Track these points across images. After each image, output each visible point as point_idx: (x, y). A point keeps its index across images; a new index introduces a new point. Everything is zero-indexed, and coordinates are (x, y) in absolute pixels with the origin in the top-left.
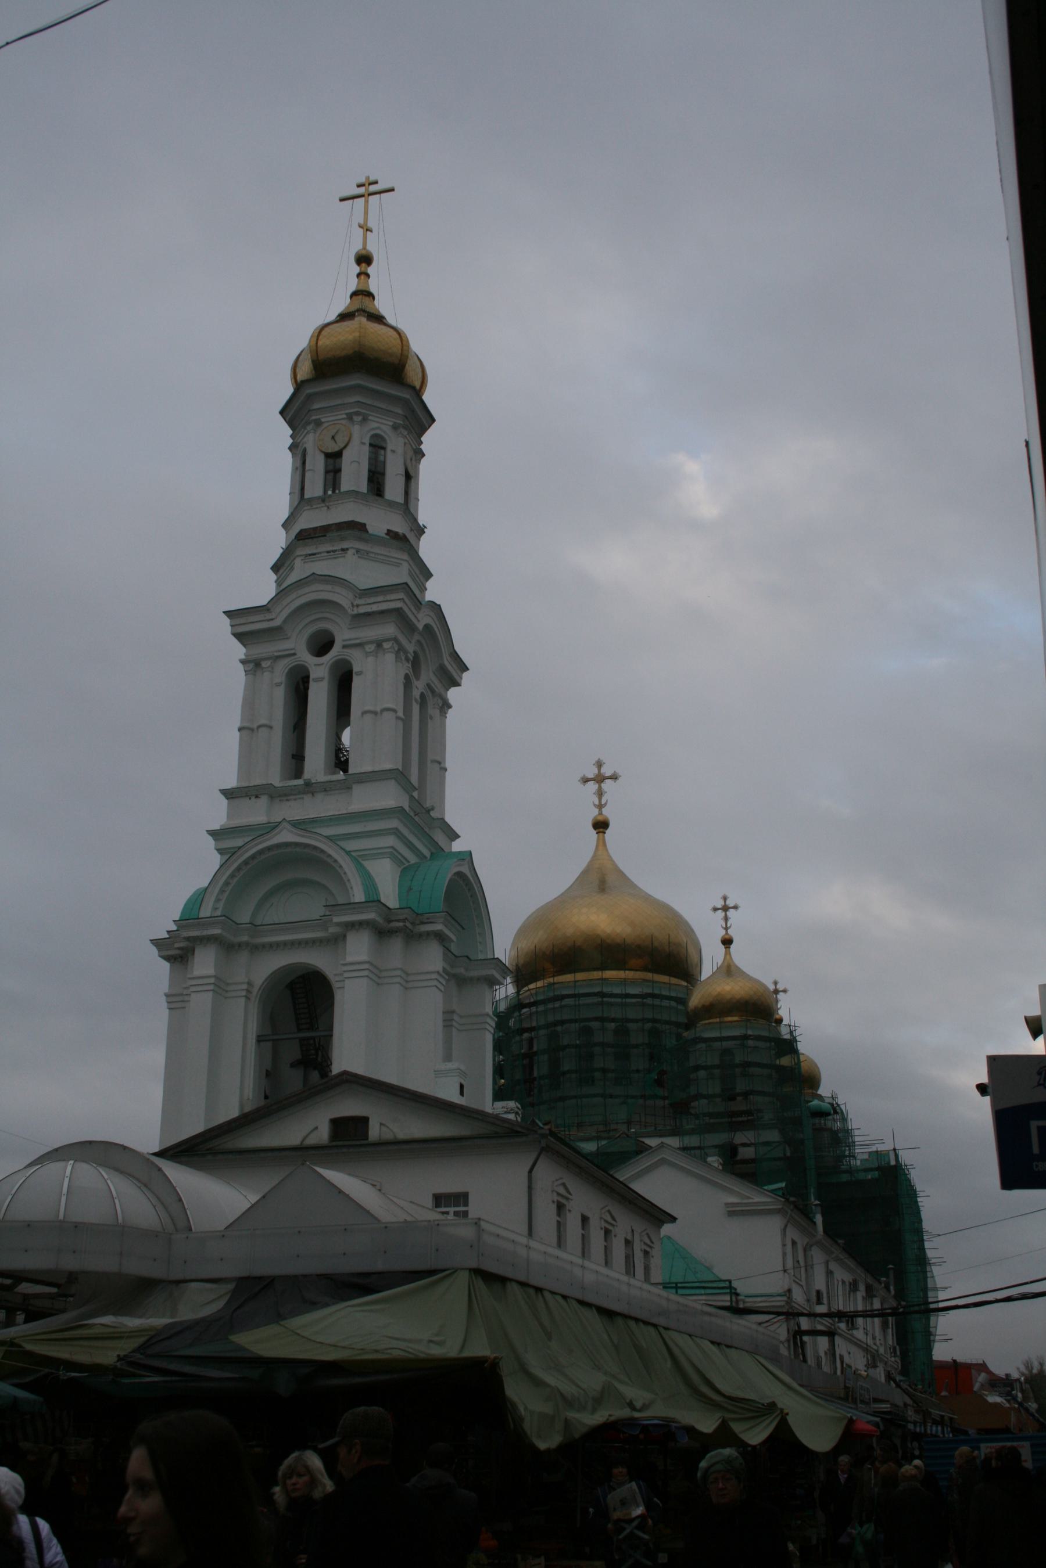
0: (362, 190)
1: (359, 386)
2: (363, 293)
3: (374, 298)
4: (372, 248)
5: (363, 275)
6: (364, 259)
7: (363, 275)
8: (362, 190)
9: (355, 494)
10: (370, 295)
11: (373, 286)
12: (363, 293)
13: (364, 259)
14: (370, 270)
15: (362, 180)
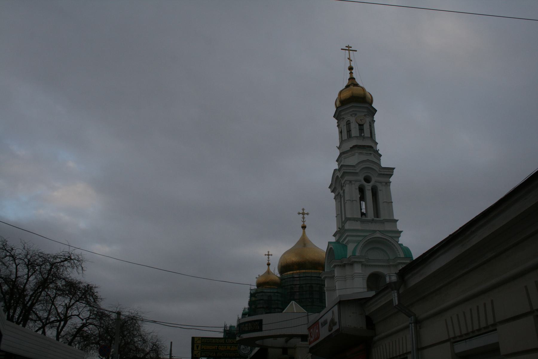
0: (347, 48)
1: (353, 106)
2: (352, 79)
3: (355, 79)
4: (353, 65)
5: (351, 73)
6: (351, 68)
7: (351, 73)
8: (347, 48)
9: (357, 137)
10: (354, 79)
11: (354, 76)
12: (352, 79)
13: (351, 68)
14: (353, 71)
15: (347, 46)
